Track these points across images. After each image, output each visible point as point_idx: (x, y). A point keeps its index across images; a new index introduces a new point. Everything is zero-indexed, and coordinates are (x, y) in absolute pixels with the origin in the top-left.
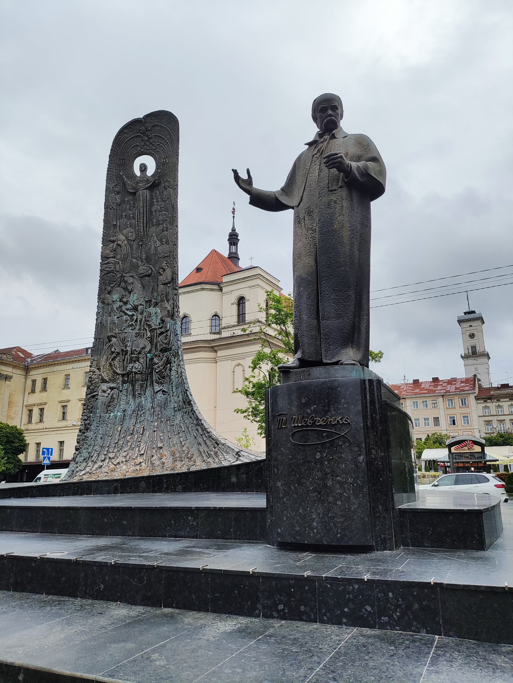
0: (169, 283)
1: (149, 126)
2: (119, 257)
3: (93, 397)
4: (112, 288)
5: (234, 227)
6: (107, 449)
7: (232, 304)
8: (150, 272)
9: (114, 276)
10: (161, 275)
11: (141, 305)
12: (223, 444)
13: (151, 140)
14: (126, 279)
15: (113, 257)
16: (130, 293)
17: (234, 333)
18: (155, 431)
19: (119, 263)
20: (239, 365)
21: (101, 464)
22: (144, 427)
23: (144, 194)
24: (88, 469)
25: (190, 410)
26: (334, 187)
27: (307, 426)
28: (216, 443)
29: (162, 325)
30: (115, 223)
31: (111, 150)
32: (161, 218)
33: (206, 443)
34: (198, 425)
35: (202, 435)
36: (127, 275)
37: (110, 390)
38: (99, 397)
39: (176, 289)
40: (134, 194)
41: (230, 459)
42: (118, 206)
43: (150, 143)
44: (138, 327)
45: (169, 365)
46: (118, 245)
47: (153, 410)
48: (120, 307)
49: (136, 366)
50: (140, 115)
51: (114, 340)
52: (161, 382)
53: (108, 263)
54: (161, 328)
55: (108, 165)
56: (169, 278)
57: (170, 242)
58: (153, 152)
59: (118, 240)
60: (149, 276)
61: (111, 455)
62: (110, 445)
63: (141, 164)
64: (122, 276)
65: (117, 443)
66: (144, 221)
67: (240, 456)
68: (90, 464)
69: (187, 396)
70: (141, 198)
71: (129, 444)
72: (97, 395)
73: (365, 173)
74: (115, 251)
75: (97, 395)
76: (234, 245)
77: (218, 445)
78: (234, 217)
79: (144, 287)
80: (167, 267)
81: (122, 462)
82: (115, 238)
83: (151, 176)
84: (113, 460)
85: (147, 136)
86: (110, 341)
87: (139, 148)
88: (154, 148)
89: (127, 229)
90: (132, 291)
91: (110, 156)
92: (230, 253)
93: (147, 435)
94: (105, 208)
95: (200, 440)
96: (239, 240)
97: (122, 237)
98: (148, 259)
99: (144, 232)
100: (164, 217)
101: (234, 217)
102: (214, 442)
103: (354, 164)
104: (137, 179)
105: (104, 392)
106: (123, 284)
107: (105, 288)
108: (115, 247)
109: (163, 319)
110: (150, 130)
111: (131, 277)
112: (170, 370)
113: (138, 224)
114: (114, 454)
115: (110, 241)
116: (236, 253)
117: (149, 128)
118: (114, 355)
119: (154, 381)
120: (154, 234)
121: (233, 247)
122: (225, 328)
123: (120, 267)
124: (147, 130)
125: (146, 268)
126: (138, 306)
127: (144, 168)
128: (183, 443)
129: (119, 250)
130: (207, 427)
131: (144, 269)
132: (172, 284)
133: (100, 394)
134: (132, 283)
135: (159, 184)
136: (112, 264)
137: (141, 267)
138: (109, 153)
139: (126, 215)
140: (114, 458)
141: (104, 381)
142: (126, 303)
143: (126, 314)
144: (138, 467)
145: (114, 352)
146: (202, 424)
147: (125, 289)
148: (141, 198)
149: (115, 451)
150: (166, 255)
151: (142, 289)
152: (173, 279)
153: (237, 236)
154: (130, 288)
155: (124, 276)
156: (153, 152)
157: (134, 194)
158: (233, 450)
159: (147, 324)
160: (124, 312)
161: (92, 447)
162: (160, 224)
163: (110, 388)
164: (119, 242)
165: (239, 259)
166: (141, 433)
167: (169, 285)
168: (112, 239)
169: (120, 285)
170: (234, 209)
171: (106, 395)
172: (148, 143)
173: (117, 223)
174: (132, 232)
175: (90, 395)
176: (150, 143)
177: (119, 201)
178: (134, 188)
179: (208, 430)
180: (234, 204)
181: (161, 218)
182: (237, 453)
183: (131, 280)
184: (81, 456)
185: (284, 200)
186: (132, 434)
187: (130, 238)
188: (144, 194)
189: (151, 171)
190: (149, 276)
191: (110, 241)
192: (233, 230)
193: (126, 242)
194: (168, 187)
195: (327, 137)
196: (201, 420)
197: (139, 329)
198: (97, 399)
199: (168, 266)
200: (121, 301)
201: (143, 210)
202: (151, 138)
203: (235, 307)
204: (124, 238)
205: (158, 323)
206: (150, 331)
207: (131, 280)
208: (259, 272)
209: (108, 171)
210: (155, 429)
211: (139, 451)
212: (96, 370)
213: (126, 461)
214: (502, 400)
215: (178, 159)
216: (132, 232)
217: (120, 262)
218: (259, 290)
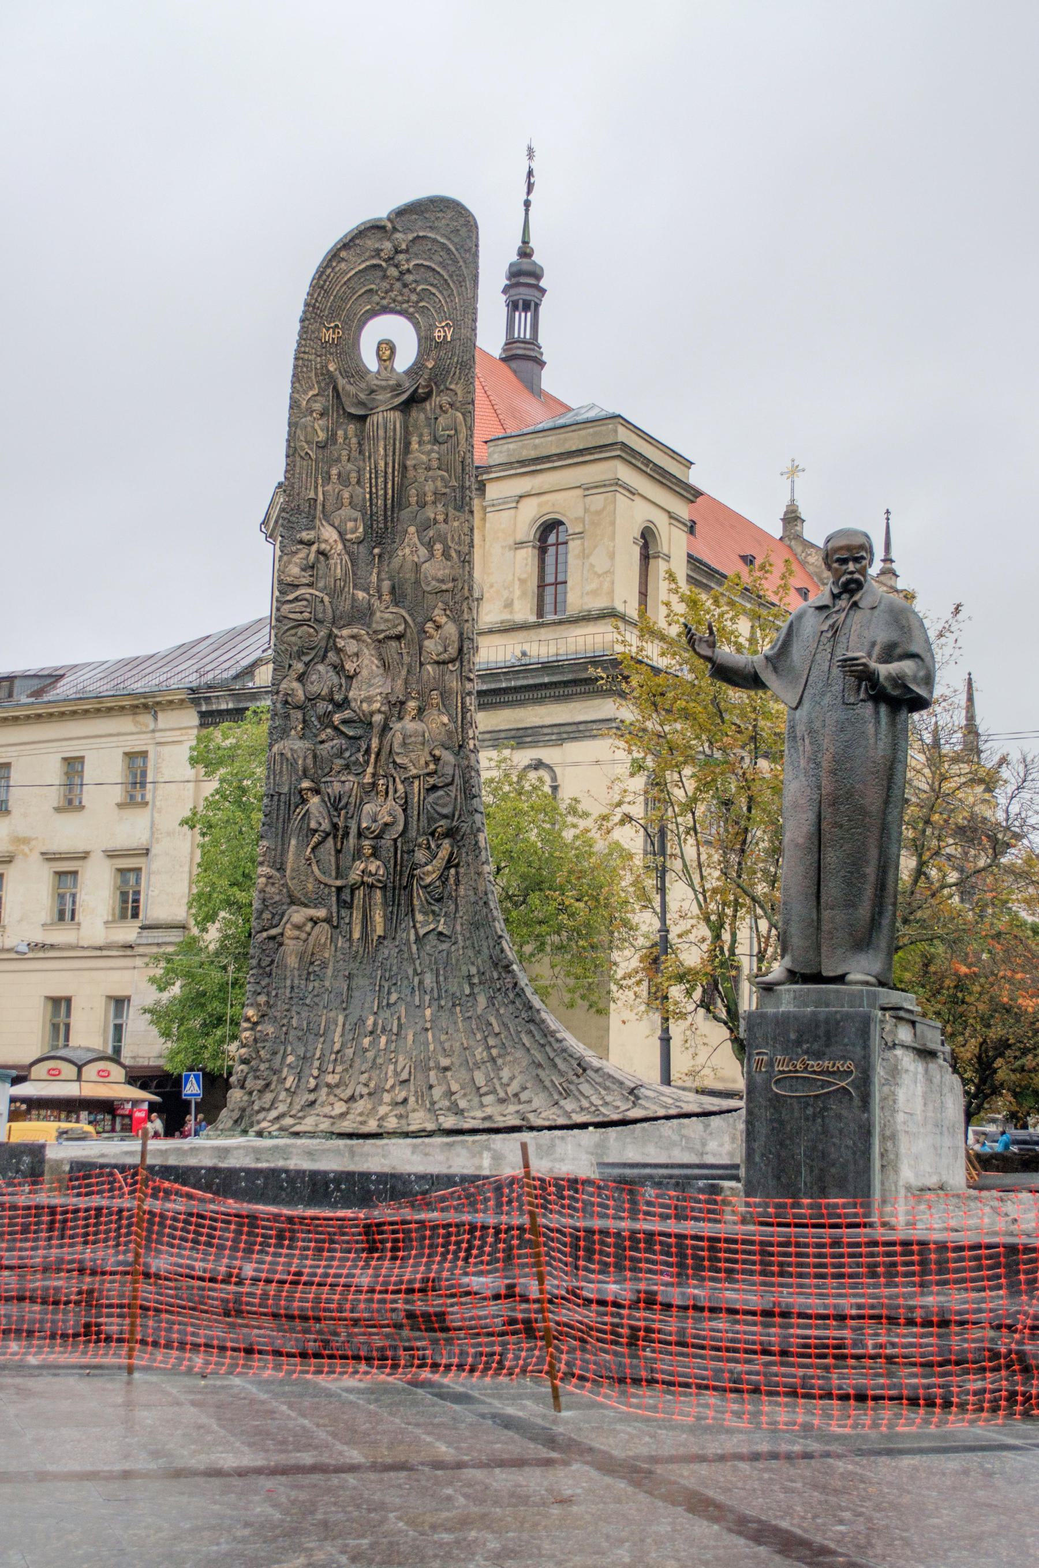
0: (452, 661)
1: (402, 238)
2: (321, 584)
3: (272, 938)
4: (307, 664)
5: (525, 242)
6: (316, 1064)
7: (520, 545)
8: (401, 628)
9: (310, 635)
10: (431, 637)
11: (379, 711)
12: (597, 1070)
13: (409, 278)
14: (341, 643)
15: (310, 585)
16: (350, 678)
17: (524, 654)
18: (427, 1030)
19: (322, 601)
20: (539, 765)
21: (312, 1097)
22: (399, 1018)
23: (386, 418)
24: (282, 1108)
25: (510, 986)
26: (852, 700)
27: (796, 1071)
28: (579, 1065)
29: (432, 767)
30: (312, 495)
31: (307, 305)
32: (429, 487)
33: (555, 1066)
34: (531, 1021)
35: (543, 1046)
36: (345, 632)
37: (310, 925)
38: (287, 941)
39: (470, 680)
40: (363, 419)
41: (618, 1103)
42: (320, 451)
43: (405, 286)
44: (370, 770)
45: (453, 871)
46: (321, 553)
47: (416, 980)
49: (372, 868)
50: (381, 210)
52: (433, 912)
53: (296, 599)
54: (428, 774)
55: (299, 345)
56: (453, 651)
58: (411, 310)
59: (318, 539)
61: (331, 1079)
62: (323, 1055)
63: (380, 343)
64: (330, 635)
65: (338, 1052)
66: (386, 494)
67: (637, 1098)
68: (283, 1095)
69: (502, 951)
71: (370, 1055)
72: (282, 934)
73: (899, 681)
74: (312, 567)
75: (282, 934)
76: (526, 307)
77: (584, 1070)
78: (527, 204)
79: (386, 666)
80: (444, 620)
81: (362, 1096)
84: (337, 1091)
85: (397, 266)
86: (304, 801)
87: (376, 298)
88: (414, 297)
90: (356, 674)
91: (302, 321)
92: (511, 342)
93: (410, 1037)
94: (287, 456)
95: (539, 1057)
96: (543, 291)
97: (329, 534)
98: (397, 595)
99: (386, 523)
100: (439, 483)
101: (527, 204)
102: (575, 1063)
103: (884, 670)
104: (369, 377)
105: (298, 927)
106: (332, 656)
107: (290, 666)
108: (312, 556)
109: (437, 752)
110: (407, 251)
111: (353, 637)
112: (457, 883)
113: (371, 499)
114: (337, 1077)
115: (301, 542)
116: (533, 342)
117: (404, 247)
118: (315, 839)
119: (417, 908)
120: (412, 529)
121: (524, 320)
122: (491, 632)
124: (401, 252)
125: (391, 616)
126: (372, 714)
127: (388, 353)
128: (500, 1061)
129: (322, 565)
130: (553, 1027)
131: (387, 620)
132: (458, 664)
133: (289, 932)
134: (357, 655)
135: (428, 395)
136: (304, 603)
137: (378, 614)
138: (298, 309)
139: (339, 475)
140: (337, 1086)
141: (293, 901)
144: (401, 1110)
145: (316, 831)
146: (543, 1021)
147: (338, 668)
148: (381, 433)
149: (339, 1069)
150: (444, 587)
151: (381, 671)
152: (460, 650)
153: (538, 277)
154: (350, 666)
155: (336, 636)
156: (411, 310)
157: (363, 419)
158: (622, 1083)
159: (394, 762)
160: (336, 728)
161: (279, 1056)
163: (311, 919)
164: (323, 546)
165: (542, 364)
166: (395, 1030)
168: (305, 535)
169: (325, 657)
170: (530, 173)
171: (304, 936)
172: (398, 285)
173: (316, 493)
174: (356, 520)
175: (265, 934)
176: (405, 286)
177: (322, 436)
178: (361, 404)
179: (558, 1035)
180: (531, 153)
181: (429, 487)
182: (632, 1091)
183: (352, 647)
184: (257, 1078)
185: (767, 676)
186: (371, 1033)
187: (349, 536)
188: (386, 418)
189: (405, 359)
190: (399, 638)
191: (301, 542)
192: (525, 252)
193: (340, 546)
194: (451, 405)
195: (843, 603)
196: (538, 1011)
197: (374, 775)
198: (281, 944)
201: (386, 464)
202: (408, 271)
203: (527, 557)
204: (335, 536)
205: (422, 762)
206: (403, 782)
207: (352, 647)
208: (624, 435)
209: (296, 359)
210: (428, 1025)
211: (396, 1074)
212: (273, 872)
213: (370, 1094)
215: (474, 329)
217: (326, 599)
218: (622, 500)
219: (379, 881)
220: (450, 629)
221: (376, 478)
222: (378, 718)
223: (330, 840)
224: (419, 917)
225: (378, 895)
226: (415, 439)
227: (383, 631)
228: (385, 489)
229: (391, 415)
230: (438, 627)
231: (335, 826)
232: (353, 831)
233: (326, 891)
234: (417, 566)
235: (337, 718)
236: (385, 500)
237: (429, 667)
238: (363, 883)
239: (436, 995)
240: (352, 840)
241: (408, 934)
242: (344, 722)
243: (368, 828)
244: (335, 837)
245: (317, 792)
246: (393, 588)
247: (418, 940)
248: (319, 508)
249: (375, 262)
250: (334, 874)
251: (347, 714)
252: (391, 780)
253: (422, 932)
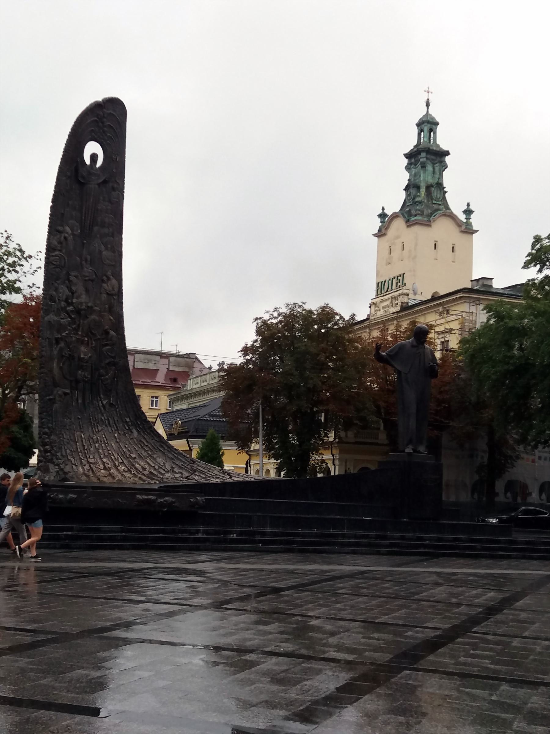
2: (64, 251)
14: (72, 278)
36: (73, 273)
48: (65, 307)
50: (100, 99)
51: (62, 344)
82: (60, 228)
97: (68, 229)
124: (104, 117)
142: (72, 304)
145: (63, 356)
154: (74, 288)
200: (66, 301)
204: (70, 232)
217: (66, 258)
227: (87, 276)
246: (91, 260)
249: (96, 118)
251: (71, 308)
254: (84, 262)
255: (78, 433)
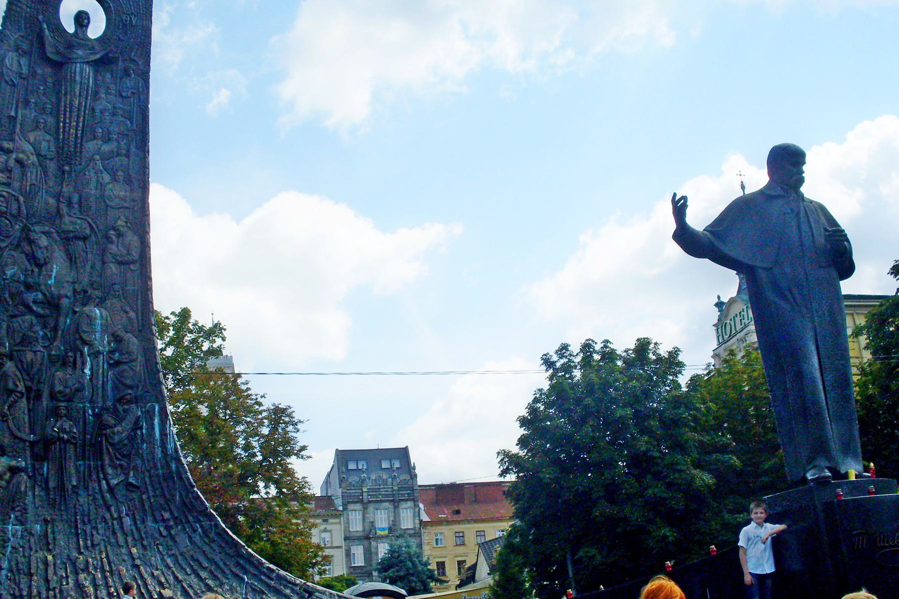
0: (133, 262)
2: (16, 185)
14: (33, 236)
30: (13, 114)
36: (37, 228)
40: (58, 65)
46: (18, 161)
49: (66, 426)
52: (120, 465)
56: (135, 254)
57: (134, 180)
60: (85, 239)
66: (77, 126)
70: (78, 78)
79: (71, 259)
80: (126, 229)
83: (97, 40)
89: (38, 133)
97: (28, 148)
99: (76, 147)
111: (44, 233)
113: (64, 127)
123: (19, 208)
126: (60, 297)
143: (31, 311)
147: (32, 258)
154: (39, 254)
162: (110, 139)
164: (21, 156)
167: (132, 267)
173: (16, 113)
174: (49, 141)
177: (25, 70)
183: (44, 241)
190: (85, 239)
199: (127, 226)
201: (80, 103)
207: (44, 241)
214: (331, 521)
216: (49, 141)
217: (22, 199)
219: (74, 438)
220: (132, 238)
221: (71, 112)
222: (65, 302)
223: (24, 400)
224: (110, 471)
225: (71, 451)
226: (103, 91)
228: (78, 122)
229: (87, 68)
230: (120, 235)
231: (29, 389)
232: (46, 394)
233: (21, 445)
234: (101, 186)
235: (30, 297)
236: (77, 130)
237: (112, 265)
238: (60, 439)
239: (136, 536)
240: (45, 402)
241: (100, 485)
242: (35, 302)
243: (60, 392)
244: (28, 399)
245: (11, 358)
247: (111, 490)
248: (18, 126)
250: (27, 430)
252: (78, 355)
253: (114, 482)
254: (64, 209)
255: (40, 554)
